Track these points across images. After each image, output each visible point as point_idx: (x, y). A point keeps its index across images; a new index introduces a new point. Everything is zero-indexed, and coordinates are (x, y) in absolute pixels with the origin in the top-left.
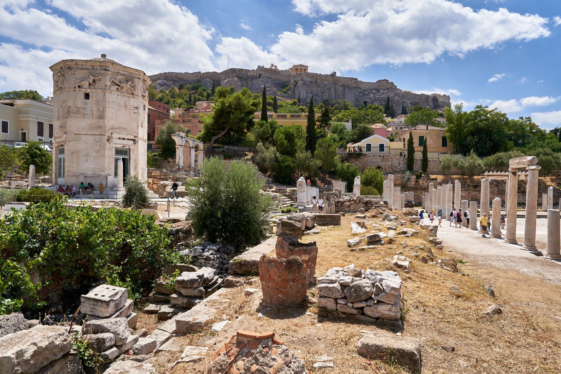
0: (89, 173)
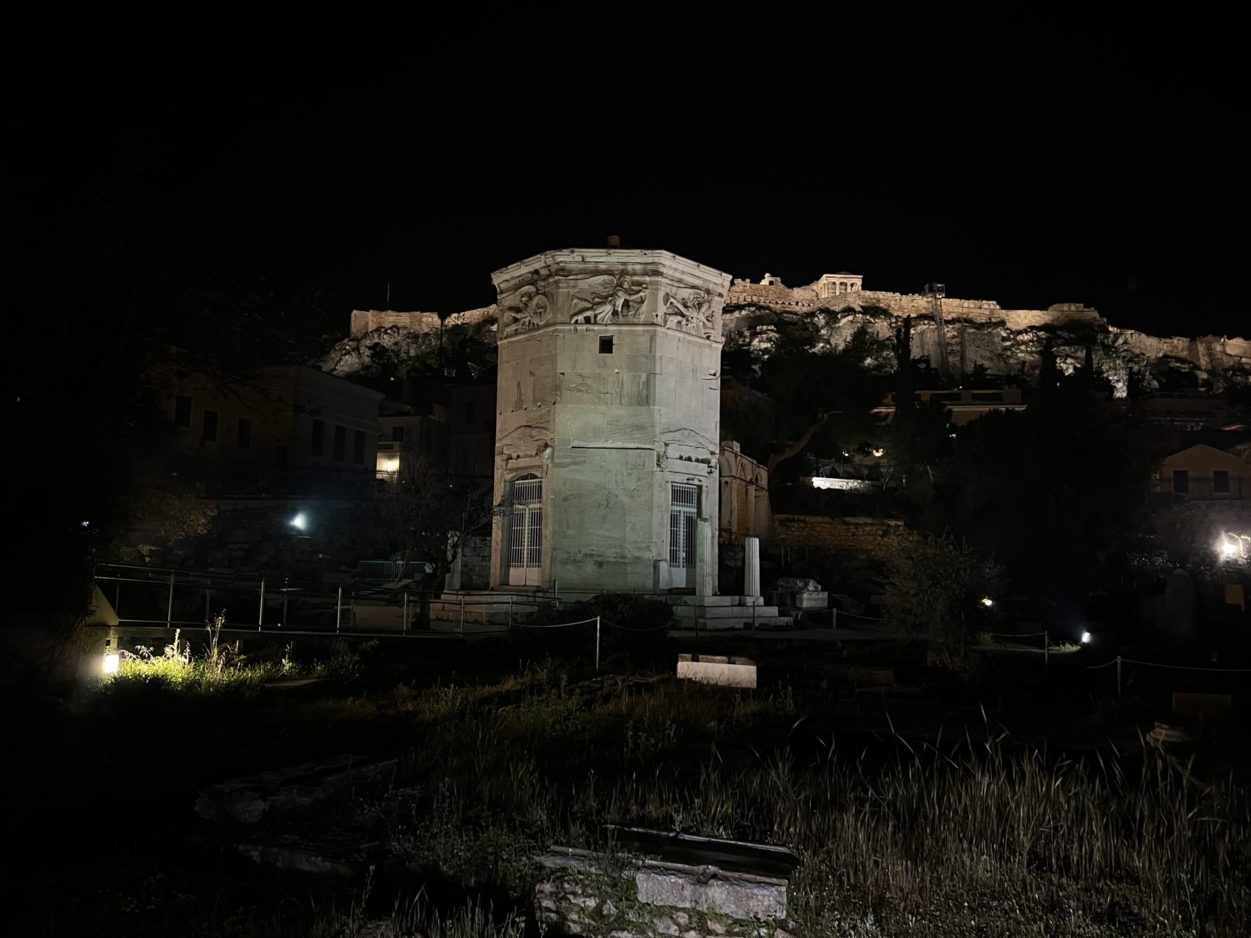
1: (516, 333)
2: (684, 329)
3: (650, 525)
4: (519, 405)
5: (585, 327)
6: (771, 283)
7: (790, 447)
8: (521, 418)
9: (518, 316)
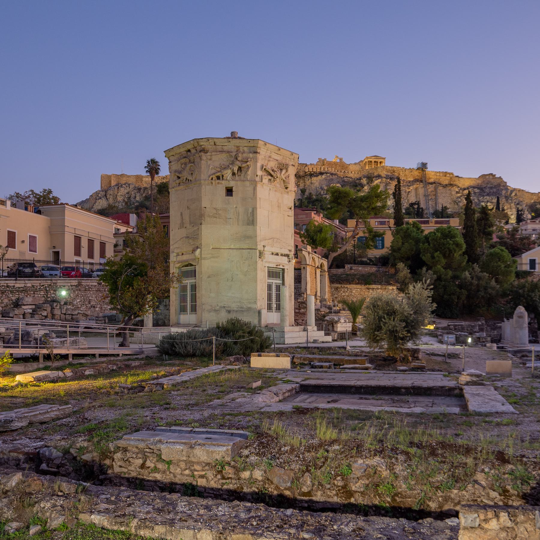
0: (234, 306)
3: (256, 290)
7: (340, 248)
8: (184, 232)
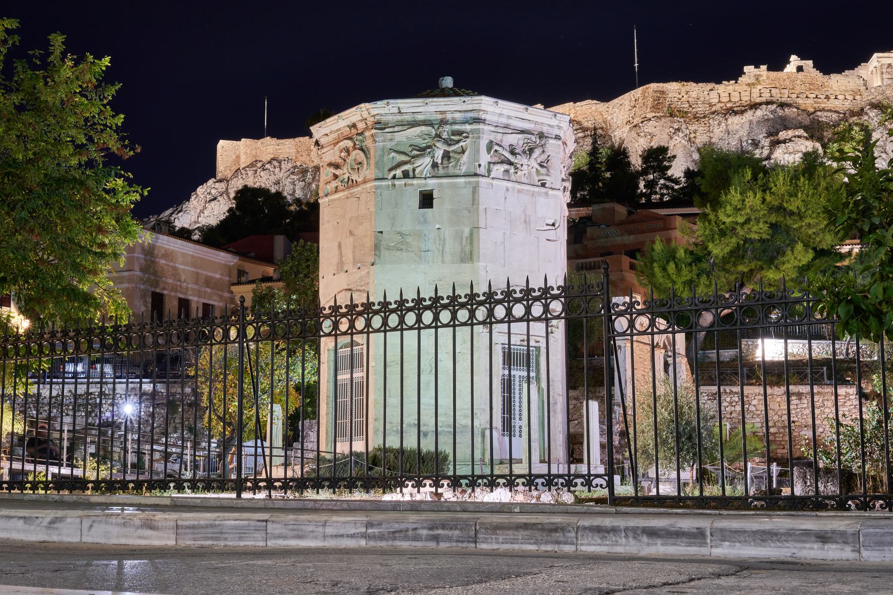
1: (336, 190)
2: (513, 178)
4: (341, 267)
5: (403, 182)
6: (800, 69)
9: (338, 172)
